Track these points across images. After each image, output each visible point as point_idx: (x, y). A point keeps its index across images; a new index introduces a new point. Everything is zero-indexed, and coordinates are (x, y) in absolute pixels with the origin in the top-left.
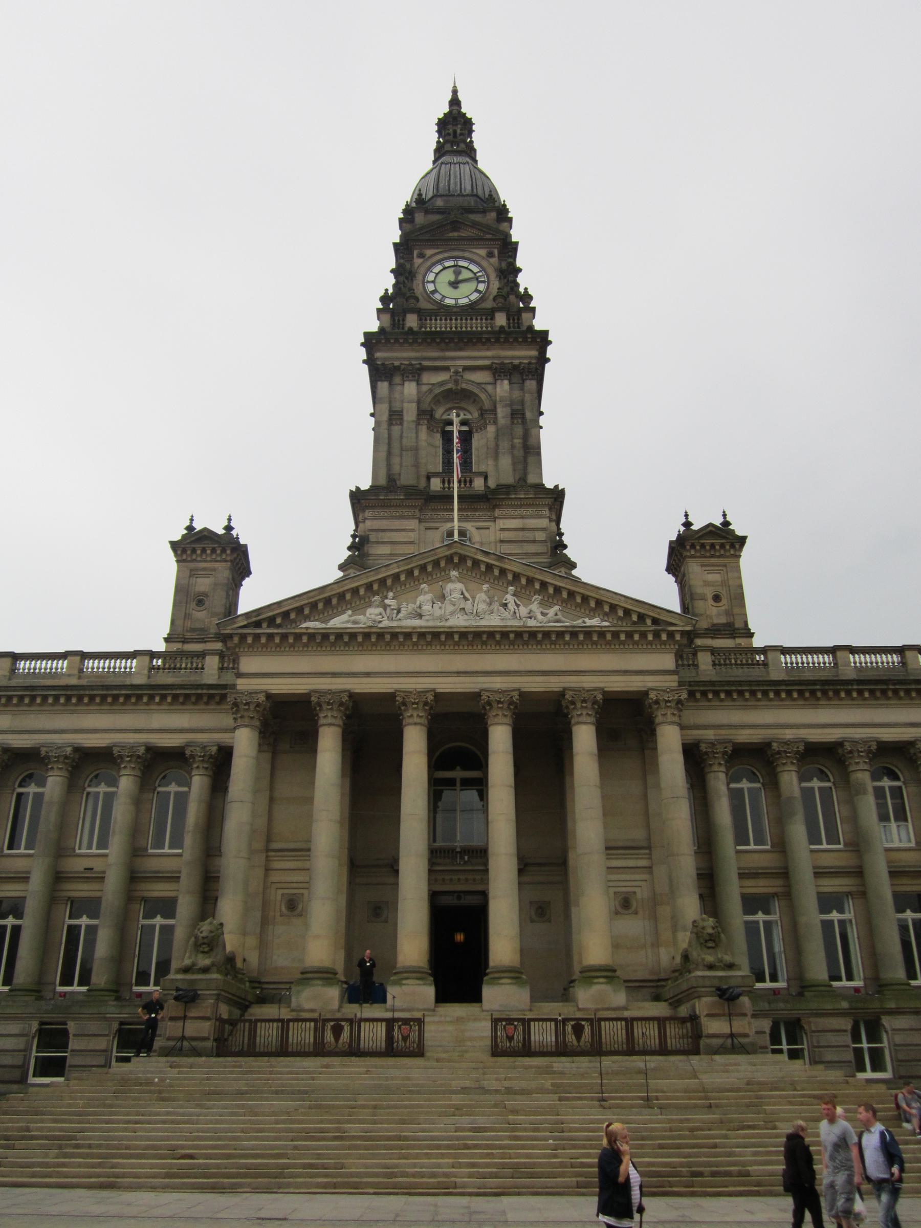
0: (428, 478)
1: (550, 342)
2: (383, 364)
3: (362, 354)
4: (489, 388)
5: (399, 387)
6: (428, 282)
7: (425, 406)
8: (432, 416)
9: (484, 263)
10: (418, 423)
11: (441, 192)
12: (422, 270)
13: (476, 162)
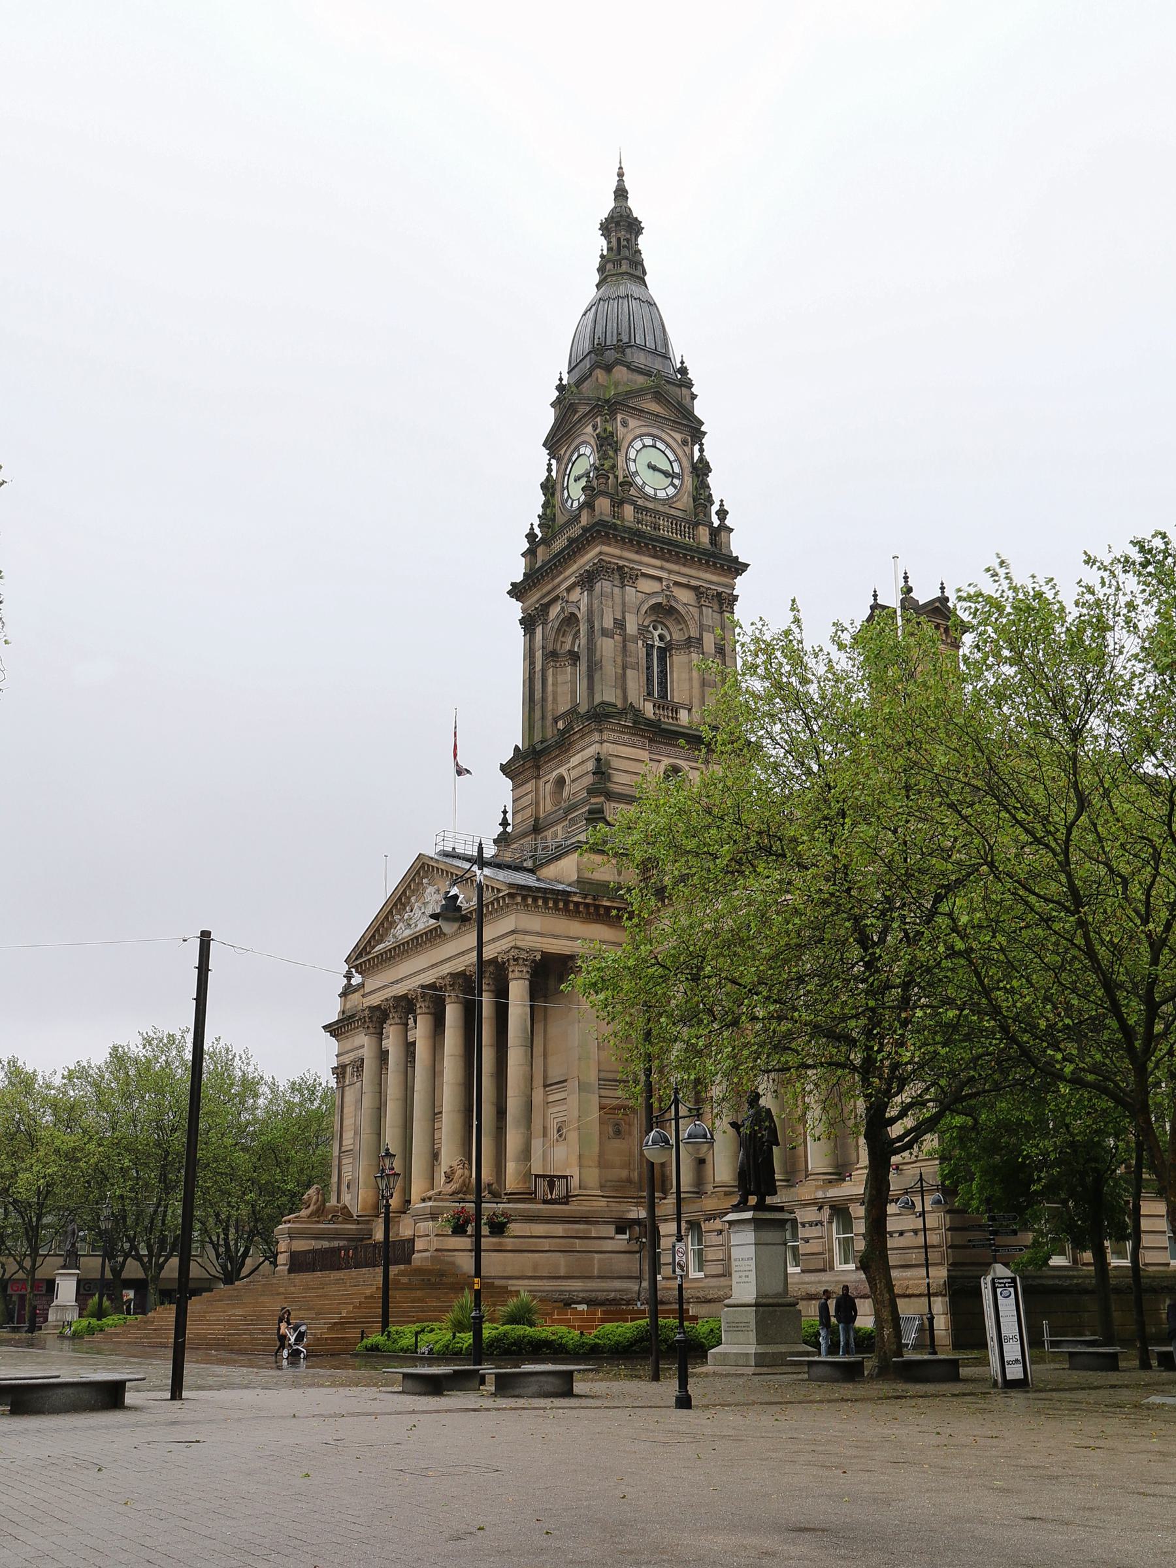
12: (625, 444)
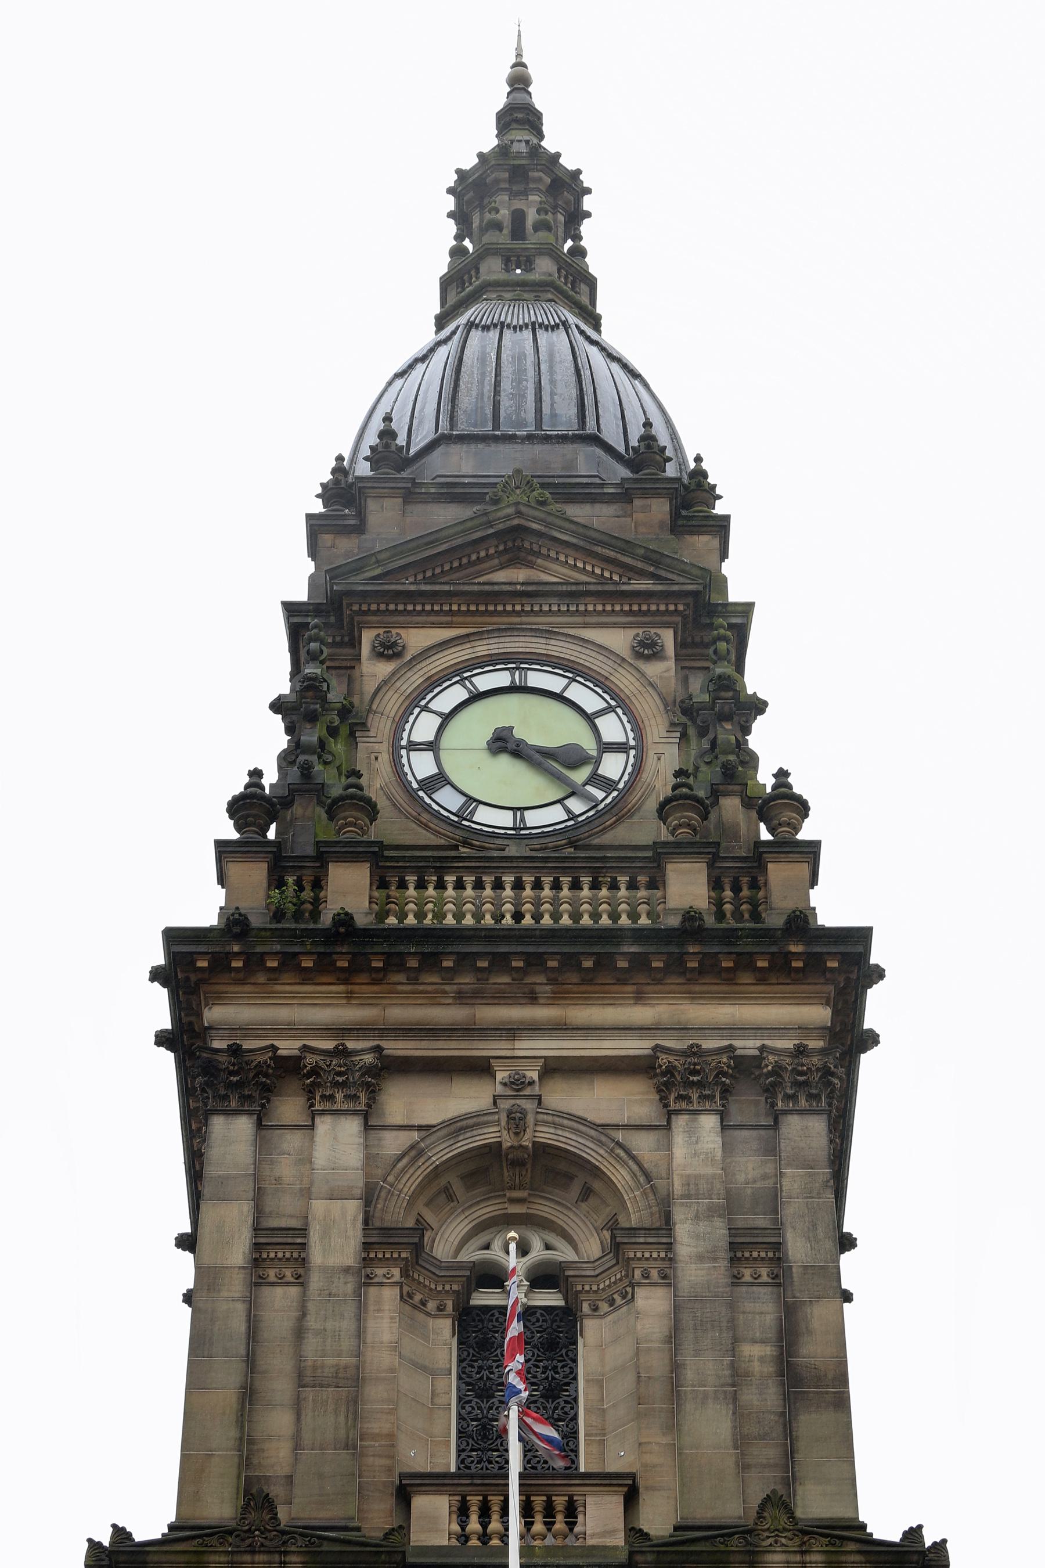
0: (404, 1493)
1: (878, 974)
2: (235, 1050)
3: (157, 1008)
4: (643, 1144)
5: (292, 1141)
6: (413, 746)
7: (396, 1213)
8: (418, 1248)
9: (625, 681)
10: (364, 1276)
11: (463, 427)
12: (392, 703)
13: (595, 322)
